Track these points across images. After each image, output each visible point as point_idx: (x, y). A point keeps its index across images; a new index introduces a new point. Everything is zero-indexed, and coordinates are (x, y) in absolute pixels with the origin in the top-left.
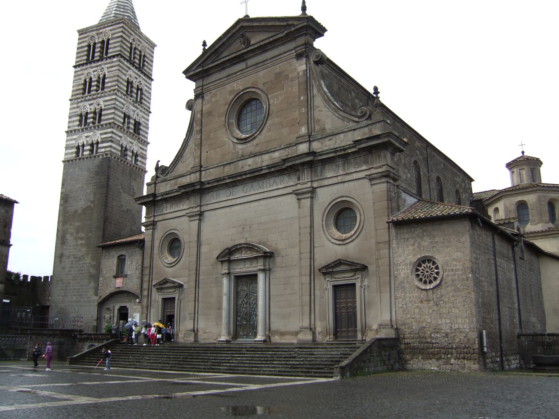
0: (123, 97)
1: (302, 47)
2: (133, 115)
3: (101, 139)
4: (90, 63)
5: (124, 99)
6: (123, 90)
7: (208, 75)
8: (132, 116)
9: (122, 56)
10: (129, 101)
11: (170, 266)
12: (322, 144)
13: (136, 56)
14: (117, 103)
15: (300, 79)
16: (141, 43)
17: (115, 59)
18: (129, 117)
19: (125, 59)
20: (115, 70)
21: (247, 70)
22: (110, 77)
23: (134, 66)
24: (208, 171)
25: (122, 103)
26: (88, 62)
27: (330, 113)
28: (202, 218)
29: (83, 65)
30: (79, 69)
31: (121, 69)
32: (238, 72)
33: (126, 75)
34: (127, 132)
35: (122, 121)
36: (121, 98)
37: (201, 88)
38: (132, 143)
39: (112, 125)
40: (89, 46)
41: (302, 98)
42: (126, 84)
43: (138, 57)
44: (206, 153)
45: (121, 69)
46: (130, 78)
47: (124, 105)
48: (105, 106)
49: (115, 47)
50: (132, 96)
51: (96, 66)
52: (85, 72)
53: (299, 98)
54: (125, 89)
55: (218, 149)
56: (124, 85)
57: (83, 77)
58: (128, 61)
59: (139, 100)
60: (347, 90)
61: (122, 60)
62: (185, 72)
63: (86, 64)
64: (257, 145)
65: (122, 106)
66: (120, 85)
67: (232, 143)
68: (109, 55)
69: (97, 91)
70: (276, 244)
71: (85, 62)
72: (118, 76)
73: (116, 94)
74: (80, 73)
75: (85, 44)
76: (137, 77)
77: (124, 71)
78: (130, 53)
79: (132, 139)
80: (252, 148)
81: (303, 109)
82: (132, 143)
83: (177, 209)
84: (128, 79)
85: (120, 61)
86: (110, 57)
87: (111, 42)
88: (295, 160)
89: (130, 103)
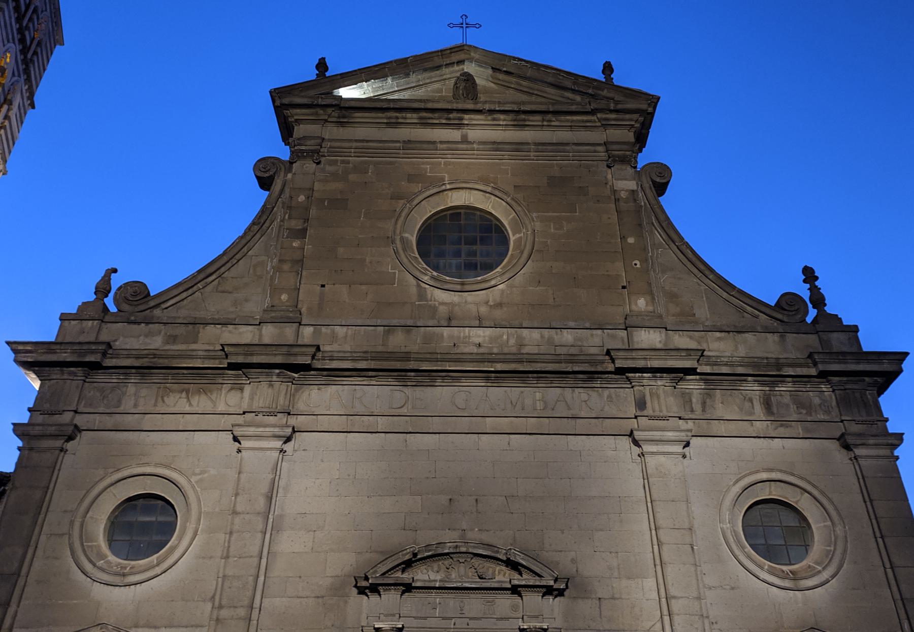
1: (624, 147)
7: (341, 124)
11: (117, 580)
12: (699, 343)
15: (622, 204)
16: (46, 10)
21: (464, 146)
24: (324, 329)
27: (703, 287)
28: (289, 447)
32: (441, 142)
37: (319, 141)
41: (631, 240)
44: (319, 288)
53: (623, 238)
55: (364, 287)
62: (276, 94)
64: (499, 305)
67: (413, 281)
70: (573, 561)
76: (16, 73)
80: (483, 310)
81: (638, 262)
83: (188, 409)
88: (645, 359)
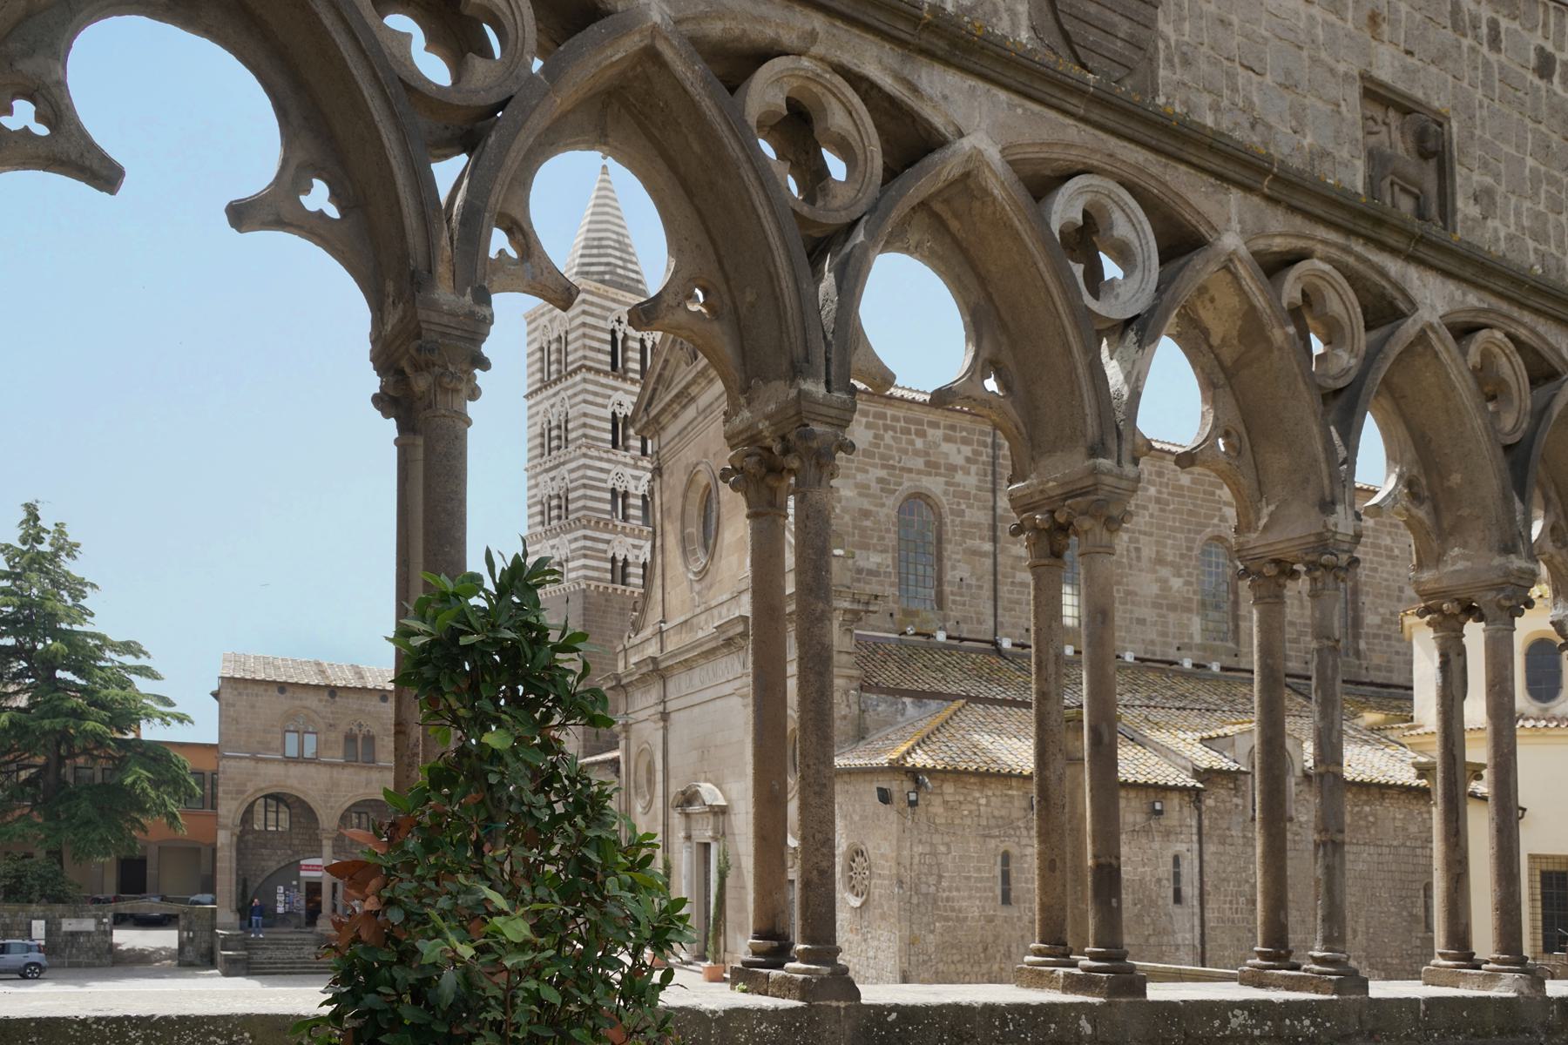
0: (605, 455)
2: (636, 488)
3: (572, 551)
4: (545, 387)
5: (609, 461)
6: (603, 440)
8: (632, 490)
9: (589, 369)
10: (623, 459)
13: (630, 354)
14: (590, 473)
17: (578, 378)
18: (626, 495)
19: (598, 371)
20: (580, 403)
22: (575, 418)
23: (625, 379)
25: (602, 470)
26: (545, 385)
29: (535, 392)
30: (532, 402)
31: (590, 398)
33: (605, 407)
34: (624, 528)
35: (608, 507)
36: (601, 459)
38: (640, 548)
39: (584, 522)
40: (542, 349)
42: (609, 426)
43: (638, 356)
45: (590, 398)
46: (617, 412)
47: (608, 471)
48: (571, 482)
49: (576, 350)
50: (627, 449)
51: (555, 395)
52: (541, 408)
54: (609, 437)
56: (604, 430)
57: (538, 419)
58: (606, 374)
59: (649, 451)
60: (908, 432)
61: (591, 376)
63: (540, 389)
65: (603, 476)
66: (593, 433)
68: (569, 369)
69: (559, 448)
71: (539, 385)
72: (585, 415)
73: (585, 455)
74: (534, 410)
75: (536, 346)
77: (600, 400)
78: (614, 354)
79: (639, 538)
82: (640, 548)
84: (614, 414)
85: (585, 380)
86: (570, 374)
87: (570, 337)
89: (625, 464)
